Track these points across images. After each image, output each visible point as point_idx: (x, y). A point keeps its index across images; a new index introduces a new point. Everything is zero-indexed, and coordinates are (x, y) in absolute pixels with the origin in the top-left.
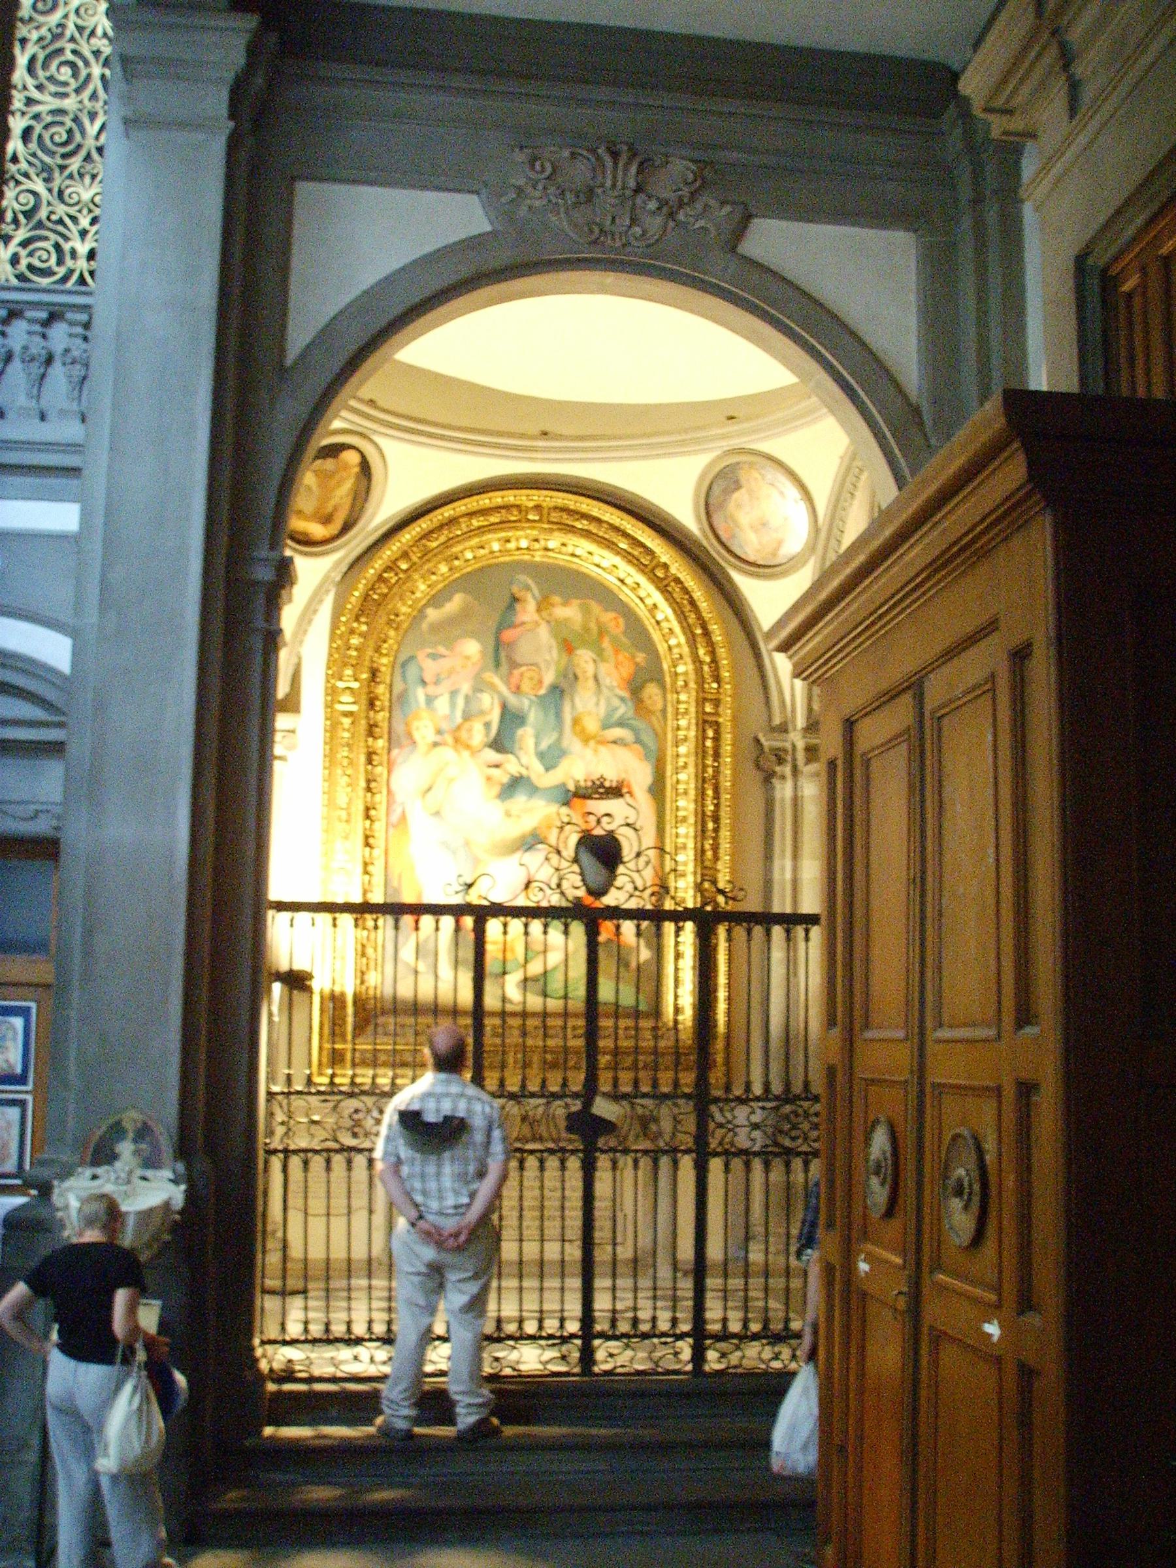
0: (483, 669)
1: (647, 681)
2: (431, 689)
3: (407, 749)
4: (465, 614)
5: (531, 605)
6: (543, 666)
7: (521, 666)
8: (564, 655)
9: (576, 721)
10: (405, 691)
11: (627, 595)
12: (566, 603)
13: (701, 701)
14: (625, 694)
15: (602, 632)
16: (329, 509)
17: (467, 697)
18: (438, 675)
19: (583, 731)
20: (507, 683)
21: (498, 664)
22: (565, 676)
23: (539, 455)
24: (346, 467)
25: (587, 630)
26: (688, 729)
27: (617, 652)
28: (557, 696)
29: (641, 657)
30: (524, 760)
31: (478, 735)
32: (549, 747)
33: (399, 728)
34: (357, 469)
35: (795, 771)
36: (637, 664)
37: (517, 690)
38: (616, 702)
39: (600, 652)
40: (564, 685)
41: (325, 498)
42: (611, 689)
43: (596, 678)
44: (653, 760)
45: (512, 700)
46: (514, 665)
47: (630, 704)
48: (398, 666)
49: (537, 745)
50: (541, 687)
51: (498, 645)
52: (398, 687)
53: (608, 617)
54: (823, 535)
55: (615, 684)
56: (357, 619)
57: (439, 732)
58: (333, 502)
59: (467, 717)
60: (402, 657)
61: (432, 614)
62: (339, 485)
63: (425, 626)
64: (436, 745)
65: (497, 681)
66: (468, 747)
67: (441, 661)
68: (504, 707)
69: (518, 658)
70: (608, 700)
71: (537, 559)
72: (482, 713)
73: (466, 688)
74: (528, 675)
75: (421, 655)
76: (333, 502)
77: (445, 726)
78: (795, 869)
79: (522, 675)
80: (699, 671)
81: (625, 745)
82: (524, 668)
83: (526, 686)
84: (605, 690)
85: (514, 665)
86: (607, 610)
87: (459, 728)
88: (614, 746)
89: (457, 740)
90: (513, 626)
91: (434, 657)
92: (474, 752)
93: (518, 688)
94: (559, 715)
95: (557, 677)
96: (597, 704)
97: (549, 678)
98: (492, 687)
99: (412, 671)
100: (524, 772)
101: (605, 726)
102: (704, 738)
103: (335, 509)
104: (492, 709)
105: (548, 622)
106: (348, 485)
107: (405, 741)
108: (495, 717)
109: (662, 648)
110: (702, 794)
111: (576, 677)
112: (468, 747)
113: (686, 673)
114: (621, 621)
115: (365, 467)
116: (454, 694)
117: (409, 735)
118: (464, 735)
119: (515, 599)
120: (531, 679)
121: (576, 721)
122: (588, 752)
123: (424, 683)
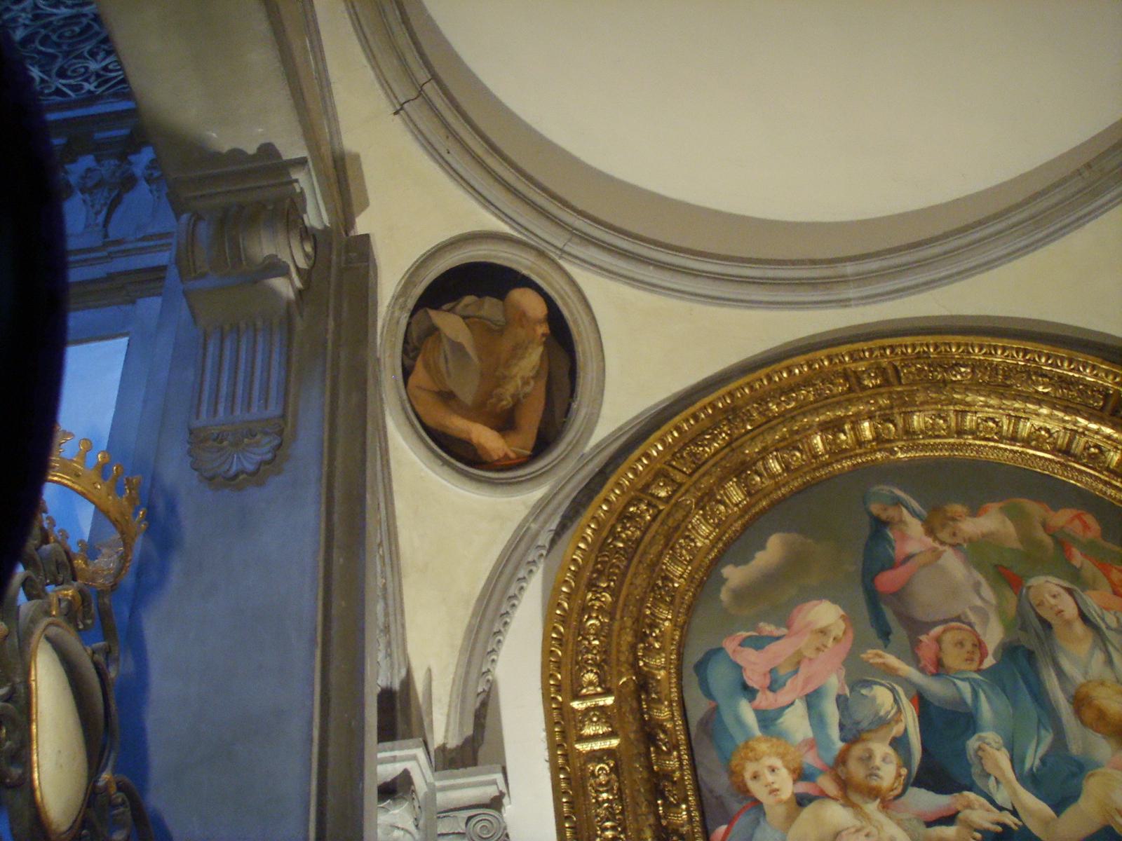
0: (859, 645)
2: (766, 700)
3: (742, 822)
4: (793, 565)
5: (915, 527)
6: (973, 618)
7: (935, 624)
8: (1011, 599)
9: (1080, 702)
10: (715, 710)
11: (1082, 477)
12: (975, 512)
15: (1062, 542)
16: (507, 402)
17: (841, 701)
18: (771, 671)
19: (1102, 715)
20: (916, 661)
21: (885, 634)
23: (852, 293)
24: (522, 316)
27: (1105, 569)
30: (1001, 797)
31: (888, 772)
32: (1043, 760)
33: (719, 783)
34: (543, 329)
37: (939, 669)
39: (1075, 577)
40: (1029, 642)
41: (494, 378)
45: (936, 688)
46: (916, 627)
48: (689, 672)
49: (1016, 761)
50: (984, 655)
51: (874, 599)
52: (698, 707)
53: (1061, 517)
56: (592, 586)
57: (801, 775)
58: (509, 389)
59: (853, 735)
60: (693, 656)
61: (734, 575)
62: (518, 351)
63: (724, 595)
64: (801, 801)
65: (892, 660)
66: (873, 793)
67: (773, 648)
68: (922, 702)
69: (920, 614)
72: (882, 723)
73: (834, 683)
74: (948, 638)
75: (730, 645)
76: (509, 389)
77: (810, 760)
79: (938, 640)
82: (938, 630)
83: (953, 658)
84: (1109, 634)
85: (916, 627)
86: (1055, 508)
87: (842, 759)
89: (845, 785)
90: (892, 564)
91: (759, 643)
92: (888, 803)
93: (939, 663)
95: (1007, 629)
97: (994, 636)
98: (889, 673)
99: (719, 676)
100: (1009, 819)
103: (517, 403)
104: (899, 711)
105: (953, 546)
106: (533, 358)
107: (736, 807)
108: (910, 721)
111: (1047, 625)
112: (873, 793)
114: (1090, 519)
115: (556, 320)
116: (812, 700)
117: (744, 792)
118: (856, 770)
119: (879, 526)
120: (961, 644)
123: (748, 691)
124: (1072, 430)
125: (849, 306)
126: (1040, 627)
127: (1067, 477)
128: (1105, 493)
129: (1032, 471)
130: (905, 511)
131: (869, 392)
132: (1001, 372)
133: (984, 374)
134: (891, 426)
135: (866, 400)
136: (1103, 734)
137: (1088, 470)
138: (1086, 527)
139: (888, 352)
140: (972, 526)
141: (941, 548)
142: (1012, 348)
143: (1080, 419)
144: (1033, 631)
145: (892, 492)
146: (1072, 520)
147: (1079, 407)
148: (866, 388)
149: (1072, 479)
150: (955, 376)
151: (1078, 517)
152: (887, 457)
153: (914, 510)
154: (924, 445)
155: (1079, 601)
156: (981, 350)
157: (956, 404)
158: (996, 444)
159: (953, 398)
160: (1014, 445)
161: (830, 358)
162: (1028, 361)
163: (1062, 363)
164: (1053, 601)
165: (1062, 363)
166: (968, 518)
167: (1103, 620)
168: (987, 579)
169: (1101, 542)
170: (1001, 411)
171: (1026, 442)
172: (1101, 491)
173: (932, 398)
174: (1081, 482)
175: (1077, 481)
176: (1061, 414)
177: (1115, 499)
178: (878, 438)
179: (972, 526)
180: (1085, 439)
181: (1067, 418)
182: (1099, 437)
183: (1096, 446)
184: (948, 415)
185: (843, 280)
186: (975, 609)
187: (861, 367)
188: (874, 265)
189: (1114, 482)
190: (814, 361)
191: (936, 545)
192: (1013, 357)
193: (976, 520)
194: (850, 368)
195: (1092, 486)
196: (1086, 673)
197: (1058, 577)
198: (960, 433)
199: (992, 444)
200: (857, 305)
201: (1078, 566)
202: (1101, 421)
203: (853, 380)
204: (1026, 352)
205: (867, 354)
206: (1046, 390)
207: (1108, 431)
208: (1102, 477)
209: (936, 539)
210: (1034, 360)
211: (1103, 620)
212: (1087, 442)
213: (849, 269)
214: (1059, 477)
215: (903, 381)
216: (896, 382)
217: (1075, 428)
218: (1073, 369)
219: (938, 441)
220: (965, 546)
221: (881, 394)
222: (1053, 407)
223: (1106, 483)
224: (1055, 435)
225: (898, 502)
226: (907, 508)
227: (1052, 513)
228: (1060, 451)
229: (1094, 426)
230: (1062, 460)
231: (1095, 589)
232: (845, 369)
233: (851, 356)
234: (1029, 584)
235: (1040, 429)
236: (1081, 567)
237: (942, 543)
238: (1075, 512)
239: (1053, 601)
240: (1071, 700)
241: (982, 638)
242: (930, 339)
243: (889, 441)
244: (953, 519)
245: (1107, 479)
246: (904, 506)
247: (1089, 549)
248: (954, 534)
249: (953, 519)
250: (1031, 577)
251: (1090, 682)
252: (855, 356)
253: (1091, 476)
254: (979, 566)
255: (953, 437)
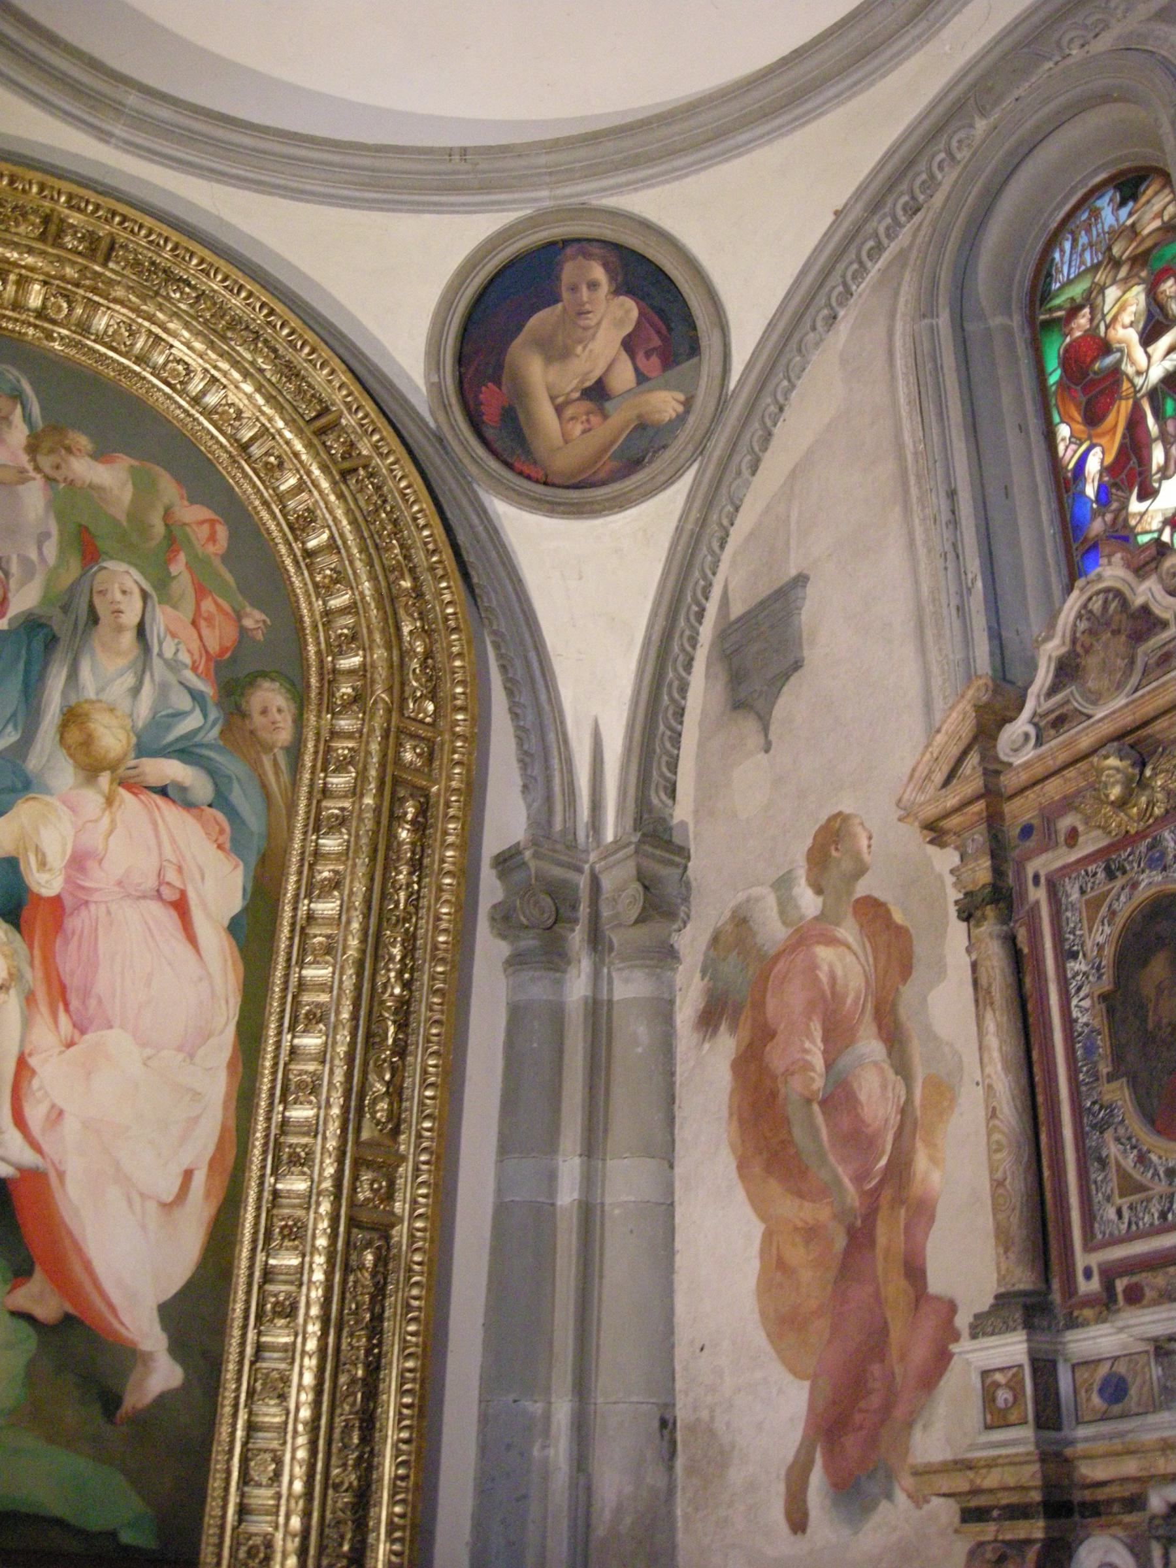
1: (264, 674)
6: (14, 568)
9: (72, 717)
12: (100, 455)
13: (394, 737)
14: (206, 688)
15: (173, 541)
19: (88, 742)
22: (65, 609)
23: (119, 130)
25: (144, 529)
26: (356, 792)
27: (201, 592)
28: (38, 644)
29: (254, 619)
35: (596, 939)
36: (243, 631)
38: (183, 701)
39: (162, 583)
40: (60, 625)
42: (173, 665)
43: (141, 631)
44: (254, 859)
47: (214, 713)
53: (192, 514)
54: (736, 409)
55: (185, 657)
70: (163, 690)
71: (57, 346)
78: (590, 1180)
80: (399, 669)
81: (188, 805)
84: (156, 662)
86: (193, 501)
88: (158, 799)
94: (32, 691)
95: (46, 600)
96: (136, 691)
101: (145, 748)
102: (395, 819)
105: (50, 480)
109: (309, 610)
110: (374, 947)
113: (363, 671)
114: (222, 532)
121: (72, 717)
122: (91, 799)
124: (263, 425)
125: (107, 142)
126: (85, 618)
127: (228, 473)
128: (258, 513)
129: (195, 445)
130: (19, 410)
131: (62, 253)
132: (228, 318)
133: (208, 309)
134: (65, 305)
135: (51, 259)
136: (75, 761)
137: (255, 479)
138: (212, 538)
139: (117, 219)
140: (85, 469)
141: (32, 474)
142: (258, 299)
143: (277, 418)
144: (74, 616)
145: (19, 381)
146: (202, 523)
147: (286, 405)
148: (62, 247)
149: (233, 478)
150: (174, 291)
151: (212, 522)
152: (39, 339)
153: (30, 415)
154: (91, 349)
155: (149, 609)
156: (224, 280)
157: (154, 323)
158: (174, 395)
159: (154, 315)
160: (193, 407)
161: (42, 188)
162: (269, 323)
163: (302, 346)
164: (118, 596)
165: (302, 346)
166: (88, 459)
167: (160, 644)
168: (61, 533)
169: (217, 562)
170: (200, 361)
171: (208, 412)
172: (255, 508)
173: (129, 300)
174: (240, 487)
175: (237, 483)
176: (260, 400)
177: (264, 524)
178: (41, 313)
179: (85, 469)
180: (272, 443)
181: (266, 409)
182: (287, 449)
183: (278, 457)
184: (139, 332)
185: (117, 109)
186: (24, 561)
187: (75, 218)
188: (164, 113)
189: (274, 506)
190: (23, 179)
191: (29, 467)
192: (254, 309)
193: (94, 463)
194: (59, 213)
195: (248, 498)
196: (101, 690)
197: (143, 573)
198: (140, 360)
199: (167, 390)
200: (117, 147)
201: (174, 573)
202: (299, 433)
203: (53, 228)
204: (272, 312)
205: (90, 208)
206: (264, 366)
207: (299, 446)
208: (266, 494)
209: (34, 460)
210: (275, 326)
211: (160, 644)
212: (273, 447)
213: (132, 99)
214: (220, 468)
215: (111, 265)
216: (100, 258)
217: (269, 425)
218: (310, 361)
219: (111, 354)
220: (62, 485)
221: (73, 263)
222: (259, 389)
223: (265, 503)
224: (245, 421)
225: (17, 396)
226: (24, 408)
227: (186, 503)
228: (237, 441)
229: (288, 435)
230: (235, 453)
231: (175, 607)
232: (52, 210)
233: (70, 196)
234: (105, 564)
235: (232, 405)
236: (175, 577)
237: (37, 469)
238: (213, 516)
239: (118, 596)
240: (65, 709)
241: (10, 595)
242: (175, 237)
243: (54, 322)
244: (69, 450)
245: (269, 499)
246: (22, 404)
247: (197, 564)
248: (58, 467)
249: (69, 450)
250: (112, 558)
251: (99, 701)
252: (74, 202)
253: (254, 486)
254: (60, 517)
255: (130, 360)
